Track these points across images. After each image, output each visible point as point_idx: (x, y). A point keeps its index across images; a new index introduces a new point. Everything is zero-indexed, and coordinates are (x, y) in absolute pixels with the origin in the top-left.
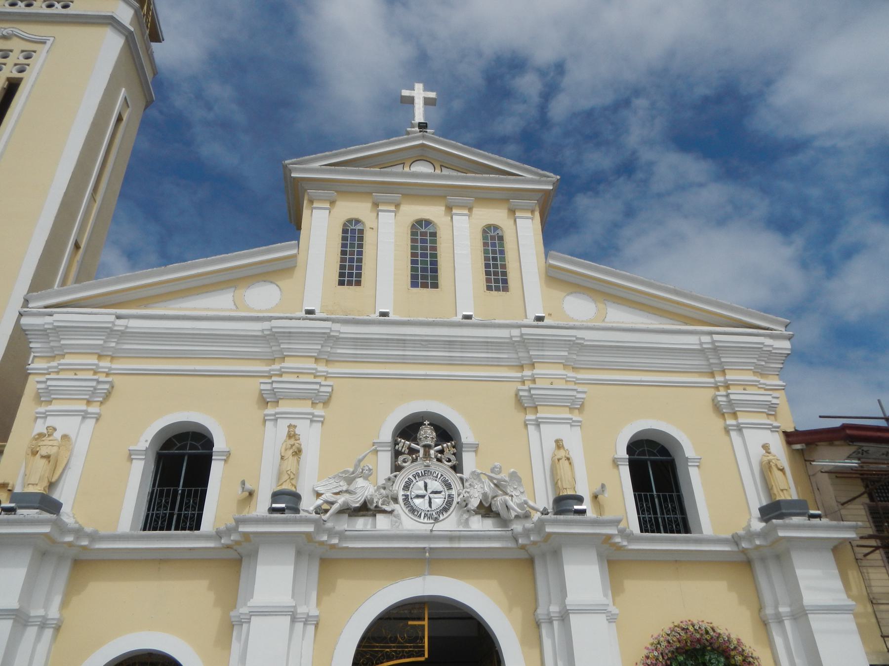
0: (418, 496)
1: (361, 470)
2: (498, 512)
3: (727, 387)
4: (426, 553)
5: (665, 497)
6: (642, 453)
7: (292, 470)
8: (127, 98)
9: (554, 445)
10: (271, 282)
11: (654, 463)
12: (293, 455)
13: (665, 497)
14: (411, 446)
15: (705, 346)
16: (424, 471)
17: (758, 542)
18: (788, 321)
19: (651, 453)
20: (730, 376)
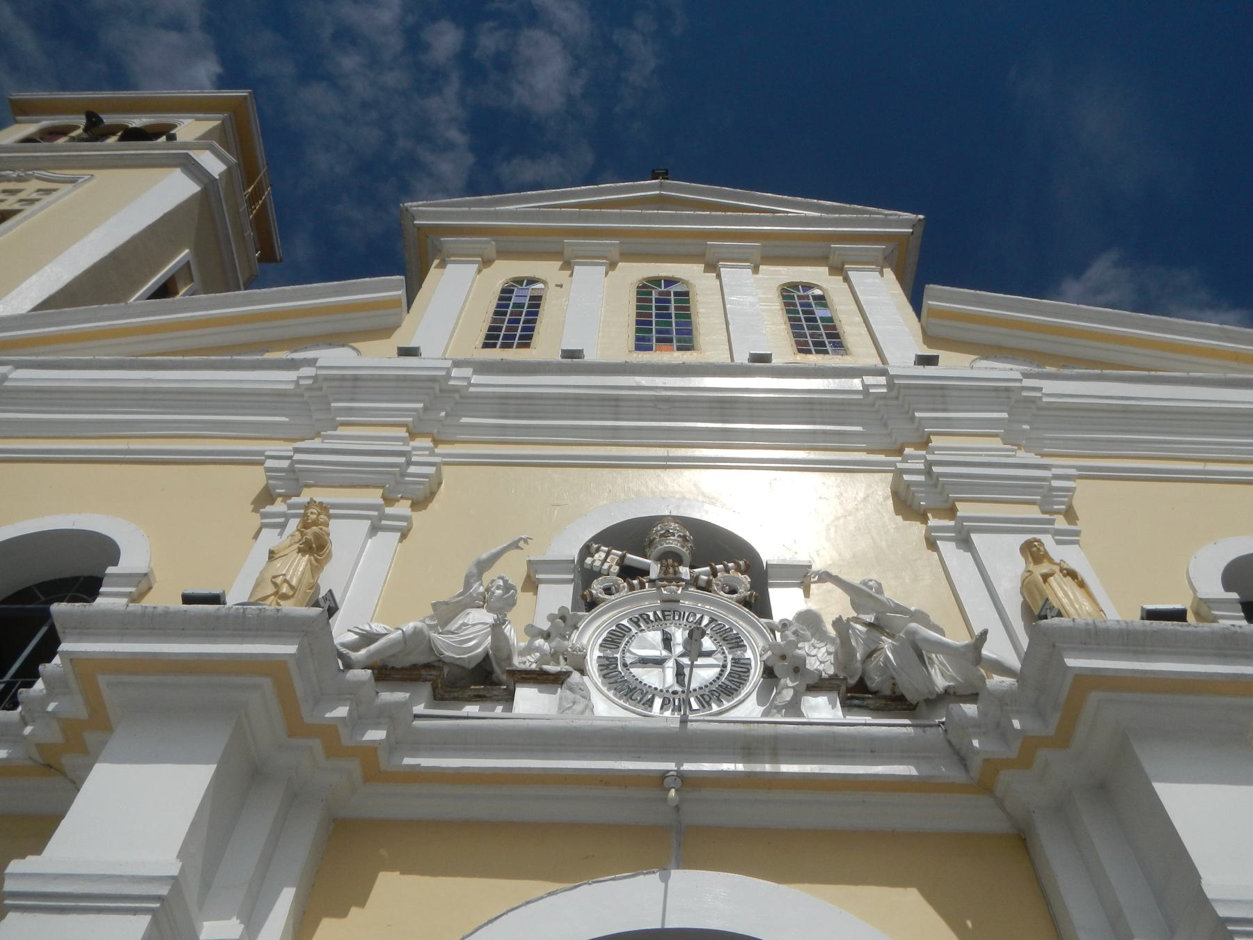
0: (644, 662)
1: (481, 589)
2: (888, 692)
4: (669, 790)
7: (288, 577)
8: (192, 263)
10: (343, 346)
12: (299, 551)
14: (627, 562)
16: (663, 612)
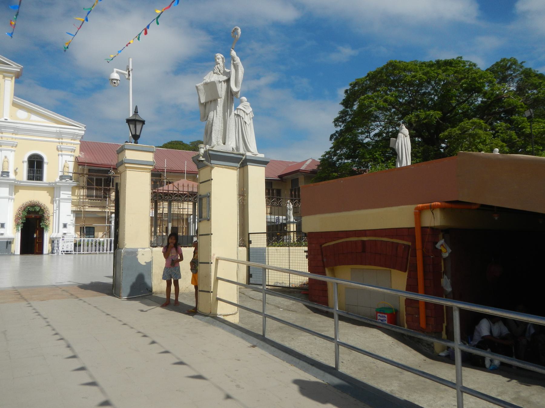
3: (62, 143)
5: (38, 170)
6: (34, 158)
9: (4, 157)
11: (37, 161)
13: (38, 170)
15: (57, 131)
17: (54, 185)
18: (85, 126)
19: (37, 159)
20: (64, 140)
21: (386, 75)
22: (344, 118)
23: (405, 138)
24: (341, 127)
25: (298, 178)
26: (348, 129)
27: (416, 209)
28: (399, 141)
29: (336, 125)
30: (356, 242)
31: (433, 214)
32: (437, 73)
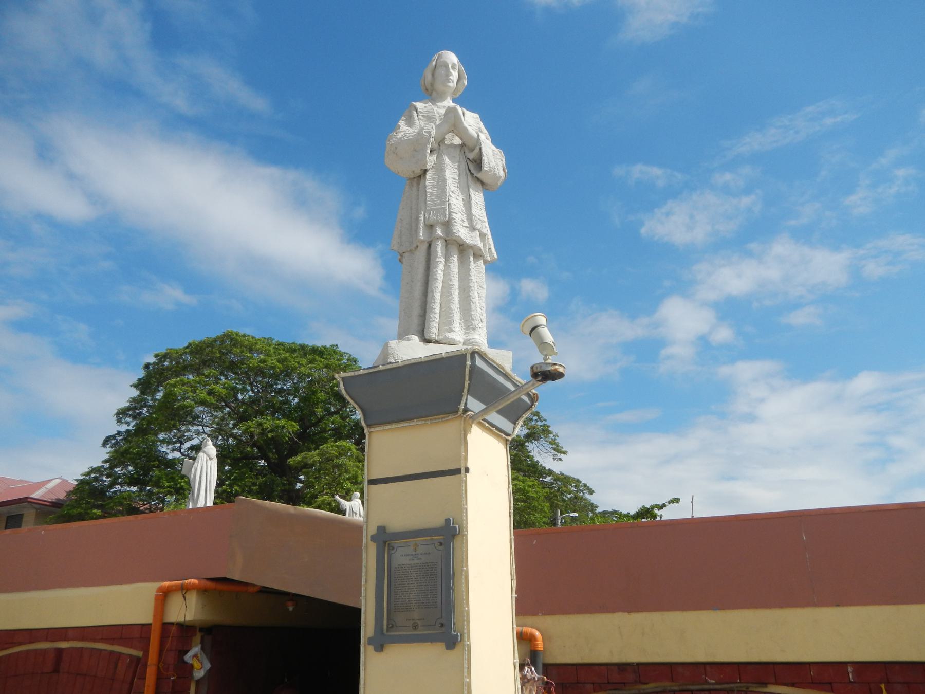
21: (220, 352)
22: (137, 411)
23: (209, 462)
24: (129, 425)
25: (22, 515)
26: (141, 431)
27: (160, 589)
28: (197, 466)
29: (119, 421)
30: (44, 652)
31: (185, 600)
32: (298, 363)
